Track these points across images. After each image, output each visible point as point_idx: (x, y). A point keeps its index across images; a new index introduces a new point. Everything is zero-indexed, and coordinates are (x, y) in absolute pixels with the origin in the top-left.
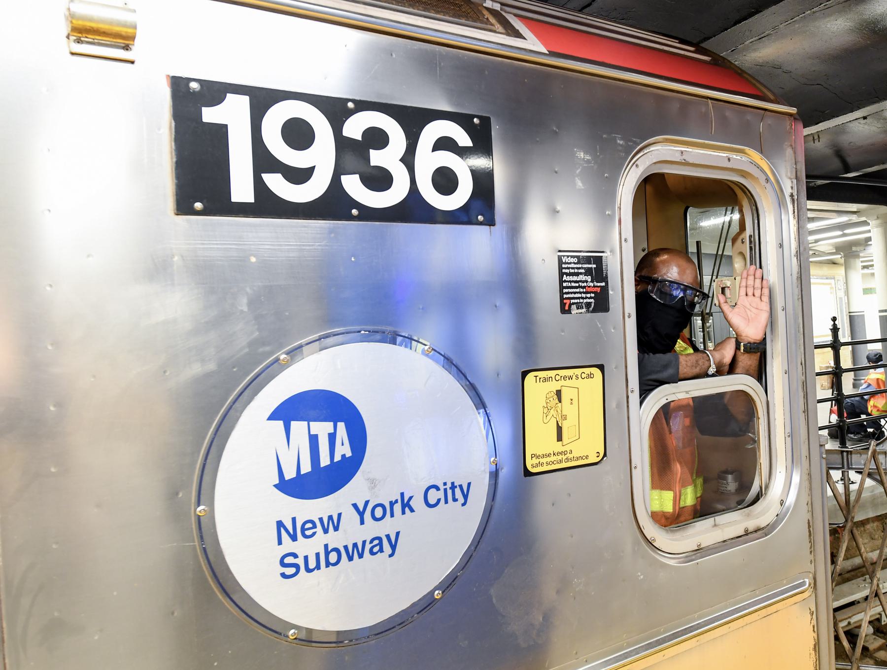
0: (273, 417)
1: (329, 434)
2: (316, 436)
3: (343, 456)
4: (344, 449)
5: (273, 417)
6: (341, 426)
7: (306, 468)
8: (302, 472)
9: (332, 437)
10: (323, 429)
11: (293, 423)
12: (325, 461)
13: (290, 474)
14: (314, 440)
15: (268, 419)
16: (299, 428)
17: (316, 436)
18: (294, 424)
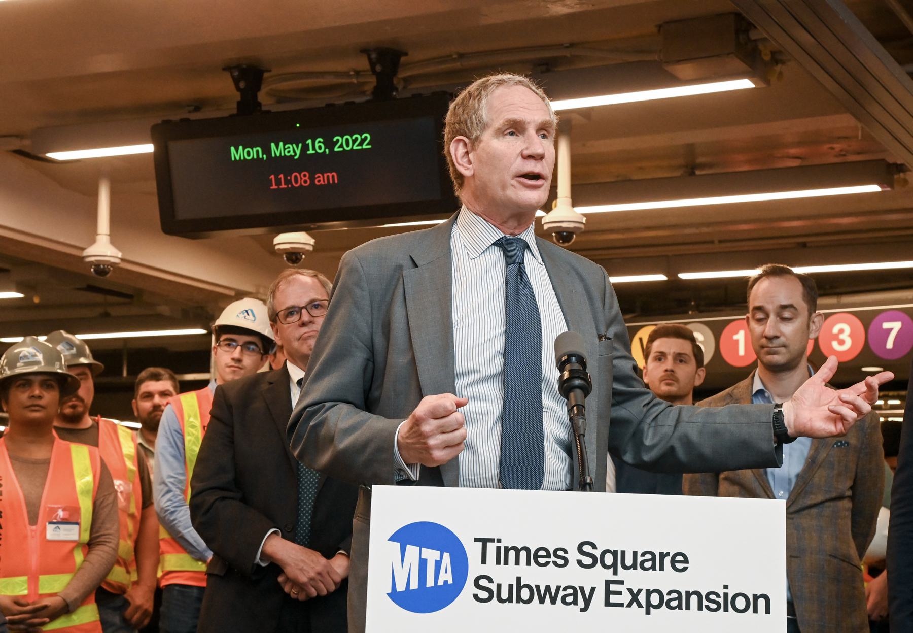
0: (393, 538)
1: (436, 561)
2: (426, 560)
3: (446, 582)
4: (446, 577)
5: (393, 538)
6: (447, 556)
7: (414, 585)
8: (411, 588)
9: (438, 564)
10: (432, 555)
11: (408, 546)
12: (430, 583)
13: (401, 588)
14: (423, 563)
15: (391, 539)
16: (412, 551)
17: (426, 560)
18: (409, 548)
